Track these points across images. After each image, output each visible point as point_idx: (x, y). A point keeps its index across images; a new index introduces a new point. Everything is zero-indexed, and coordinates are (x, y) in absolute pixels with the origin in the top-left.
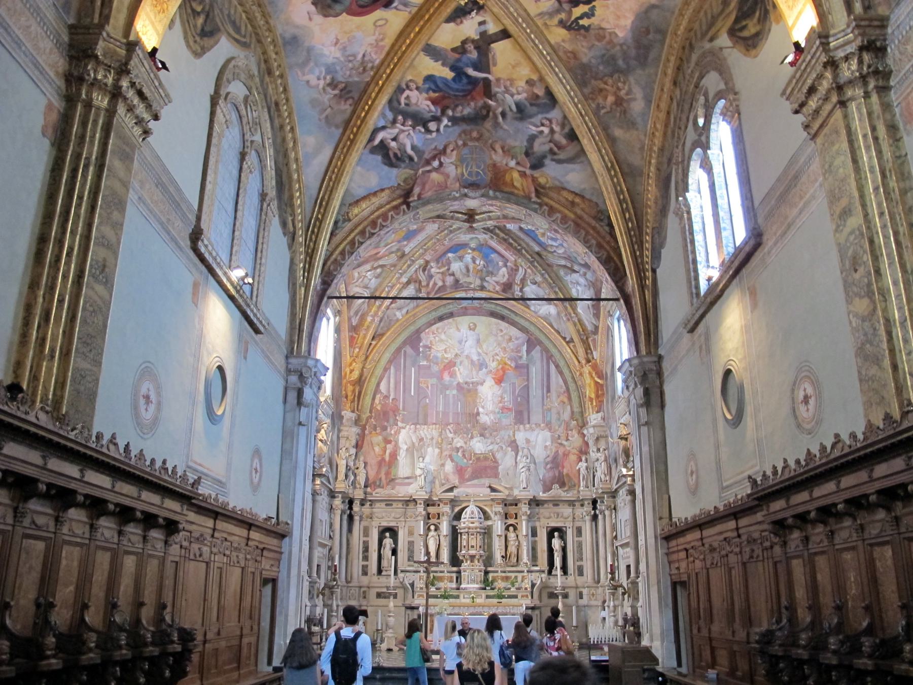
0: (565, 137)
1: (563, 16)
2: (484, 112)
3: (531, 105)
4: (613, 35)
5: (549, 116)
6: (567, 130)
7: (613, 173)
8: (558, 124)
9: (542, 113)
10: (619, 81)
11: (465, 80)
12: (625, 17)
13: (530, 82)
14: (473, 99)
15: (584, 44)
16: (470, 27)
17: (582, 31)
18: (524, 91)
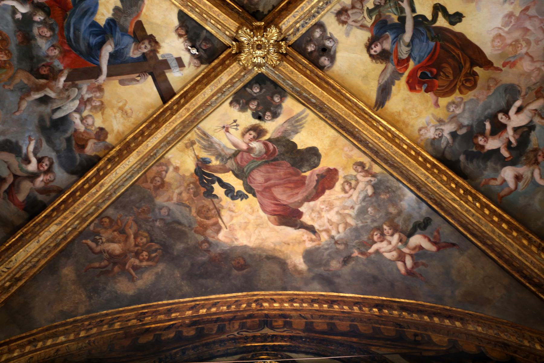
0: (28, 197)
1: (215, 162)
2: (44, 71)
3: (68, 140)
4: (216, 228)
5: (56, 168)
6: (40, 197)
7: (8, 284)
8: (47, 183)
9: (59, 157)
10: (150, 253)
11: (93, 41)
12: (250, 236)
13: (102, 133)
14: (64, 54)
15: (185, 195)
16: (173, 46)
17: (203, 190)
18: (87, 126)
